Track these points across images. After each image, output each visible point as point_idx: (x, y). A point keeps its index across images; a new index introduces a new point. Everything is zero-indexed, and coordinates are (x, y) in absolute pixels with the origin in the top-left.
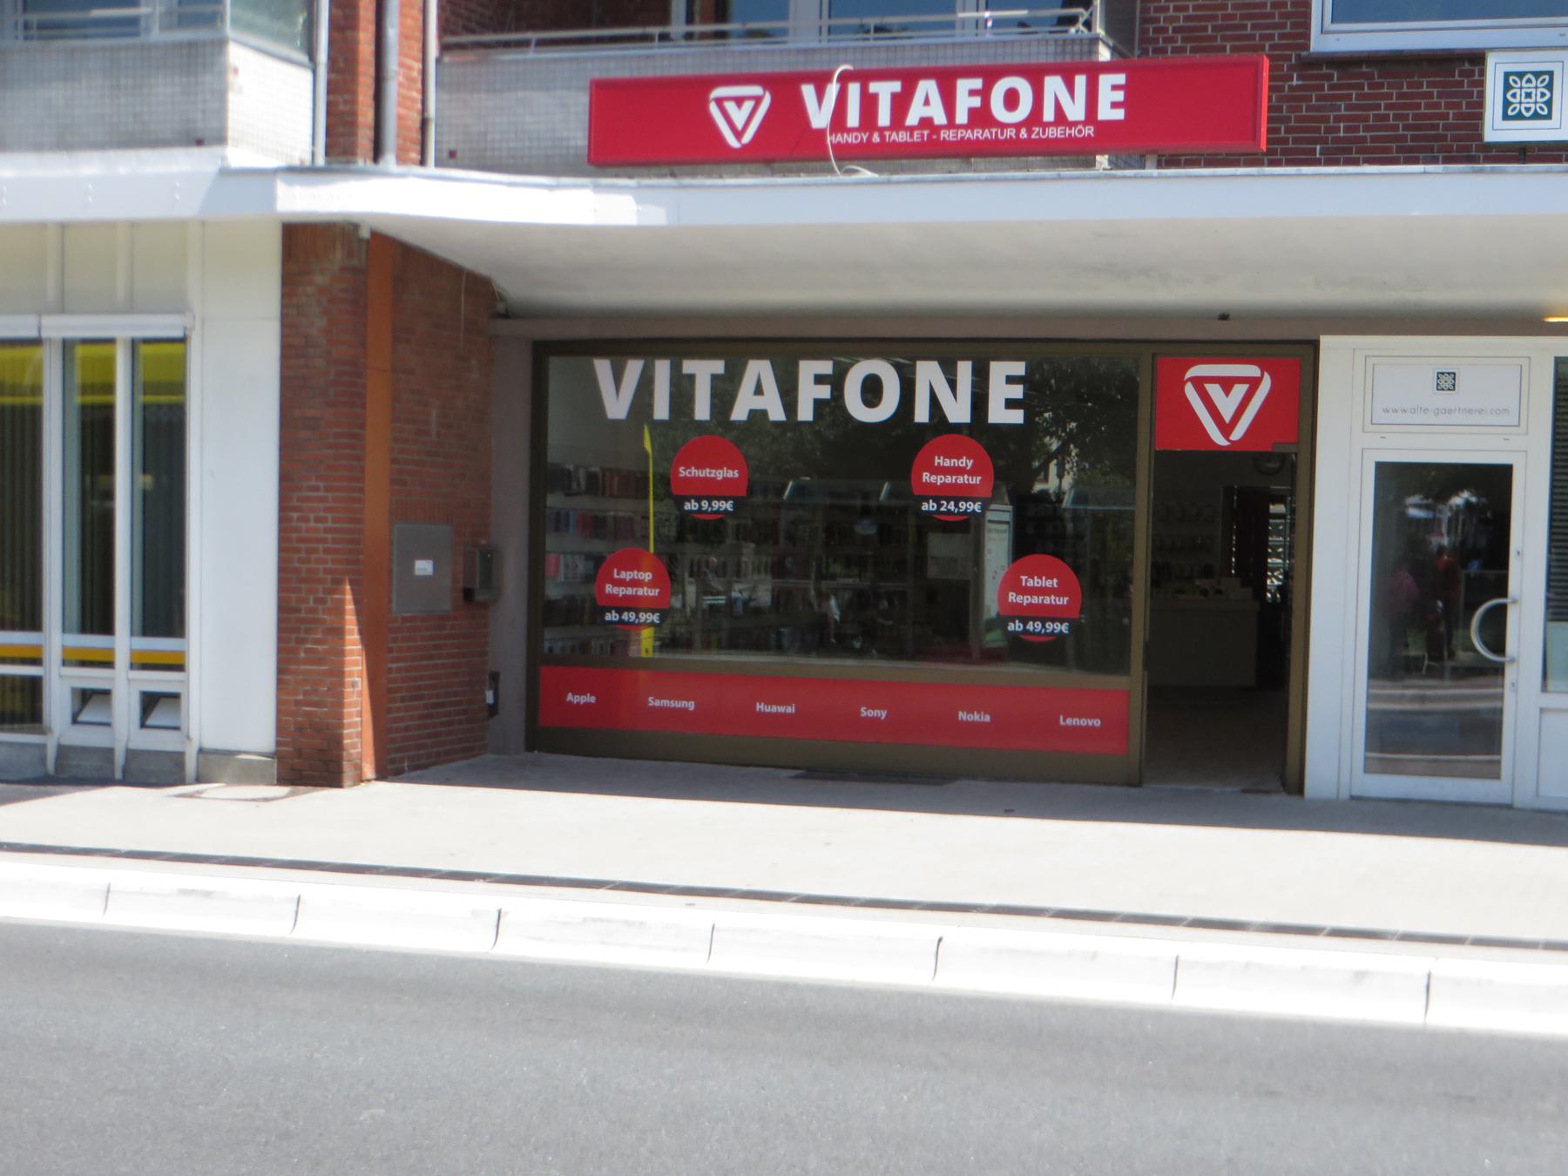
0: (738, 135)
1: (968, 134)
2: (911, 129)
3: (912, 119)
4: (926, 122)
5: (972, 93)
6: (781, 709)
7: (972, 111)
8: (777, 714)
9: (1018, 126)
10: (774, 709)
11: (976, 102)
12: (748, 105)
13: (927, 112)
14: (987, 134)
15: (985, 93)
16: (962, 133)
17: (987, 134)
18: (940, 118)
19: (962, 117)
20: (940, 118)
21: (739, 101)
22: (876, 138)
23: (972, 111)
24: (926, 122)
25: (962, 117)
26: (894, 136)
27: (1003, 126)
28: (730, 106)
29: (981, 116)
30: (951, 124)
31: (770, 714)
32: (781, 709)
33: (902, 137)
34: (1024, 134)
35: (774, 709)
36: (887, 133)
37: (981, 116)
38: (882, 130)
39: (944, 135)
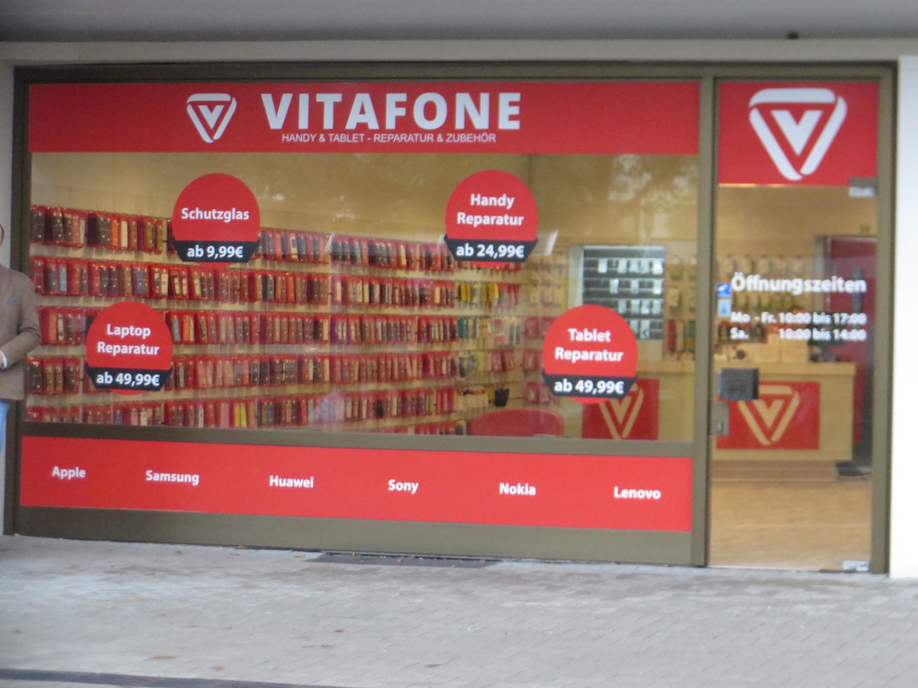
0: (211, 133)
1: (396, 138)
2: (350, 132)
3: (351, 124)
4: (362, 127)
5: (399, 105)
6: (298, 483)
7: (398, 119)
8: (294, 489)
9: (435, 132)
10: (290, 483)
11: (402, 112)
12: (219, 109)
13: (362, 119)
14: (411, 138)
15: (408, 105)
16: (390, 137)
17: (411, 138)
18: (373, 125)
19: (390, 124)
20: (373, 125)
21: (211, 105)
22: (322, 138)
23: (398, 119)
24: (362, 127)
25: (390, 124)
26: (337, 138)
27: (424, 132)
28: (204, 109)
29: (406, 124)
30: (382, 129)
31: (286, 488)
32: (298, 483)
33: (343, 138)
34: (440, 139)
35: (290, 483)
36: (331, 135)
37: (406, 124)
38: (326, 132)
39: (377, 138)
